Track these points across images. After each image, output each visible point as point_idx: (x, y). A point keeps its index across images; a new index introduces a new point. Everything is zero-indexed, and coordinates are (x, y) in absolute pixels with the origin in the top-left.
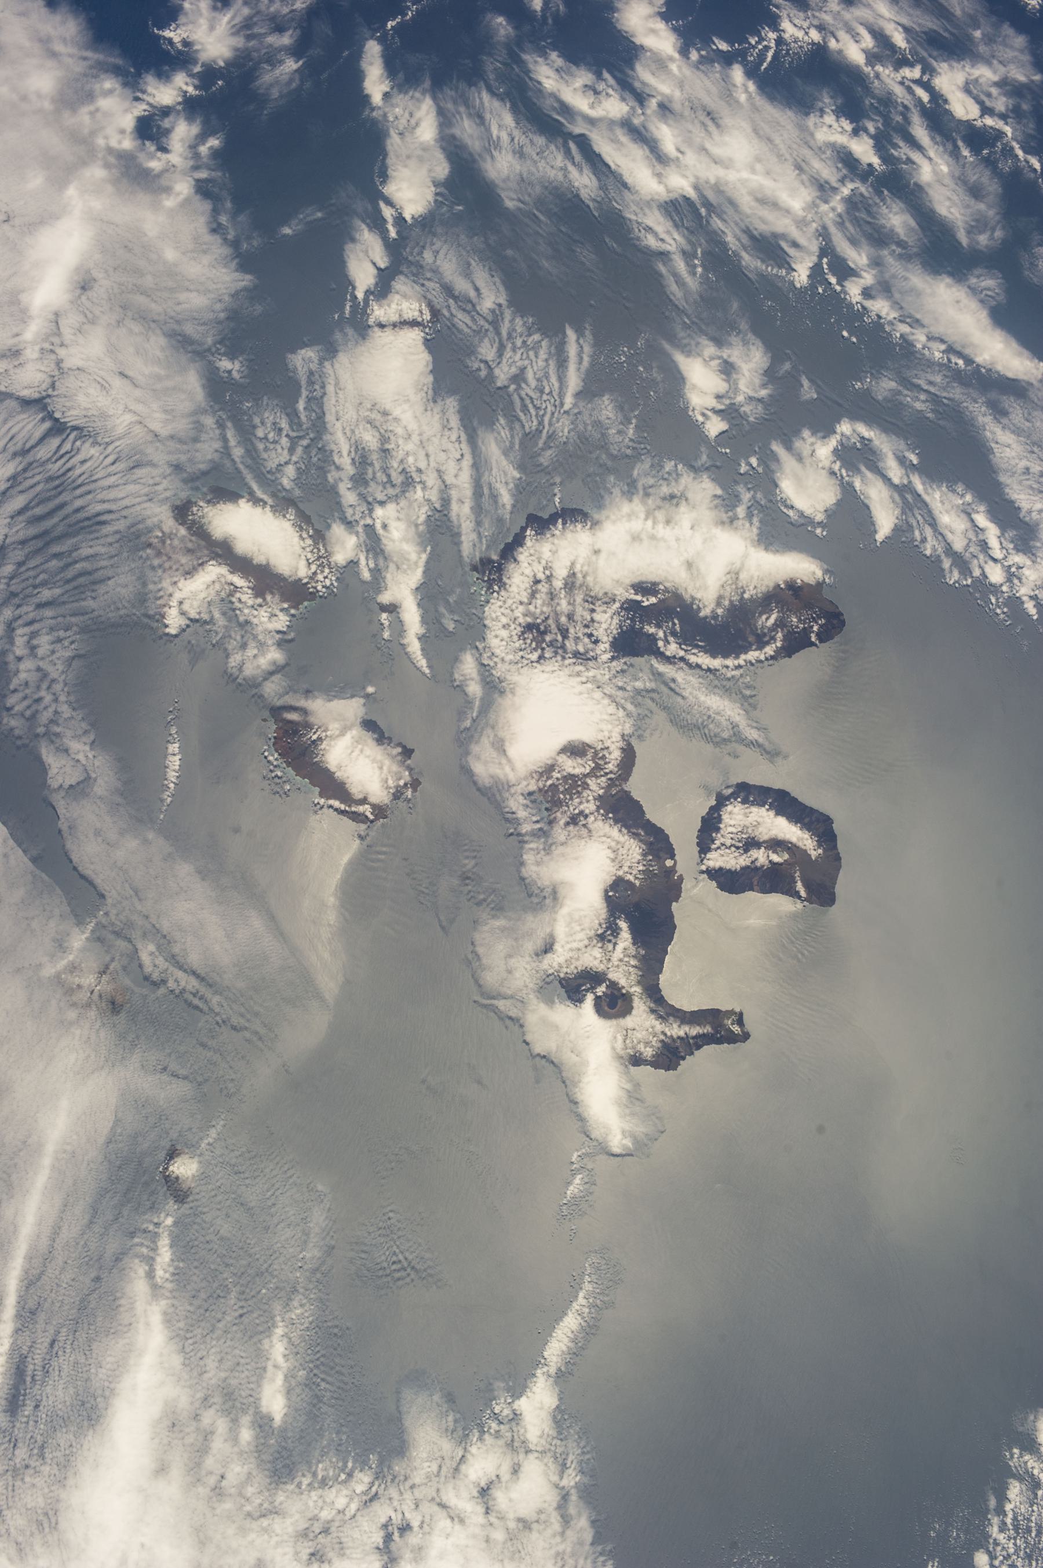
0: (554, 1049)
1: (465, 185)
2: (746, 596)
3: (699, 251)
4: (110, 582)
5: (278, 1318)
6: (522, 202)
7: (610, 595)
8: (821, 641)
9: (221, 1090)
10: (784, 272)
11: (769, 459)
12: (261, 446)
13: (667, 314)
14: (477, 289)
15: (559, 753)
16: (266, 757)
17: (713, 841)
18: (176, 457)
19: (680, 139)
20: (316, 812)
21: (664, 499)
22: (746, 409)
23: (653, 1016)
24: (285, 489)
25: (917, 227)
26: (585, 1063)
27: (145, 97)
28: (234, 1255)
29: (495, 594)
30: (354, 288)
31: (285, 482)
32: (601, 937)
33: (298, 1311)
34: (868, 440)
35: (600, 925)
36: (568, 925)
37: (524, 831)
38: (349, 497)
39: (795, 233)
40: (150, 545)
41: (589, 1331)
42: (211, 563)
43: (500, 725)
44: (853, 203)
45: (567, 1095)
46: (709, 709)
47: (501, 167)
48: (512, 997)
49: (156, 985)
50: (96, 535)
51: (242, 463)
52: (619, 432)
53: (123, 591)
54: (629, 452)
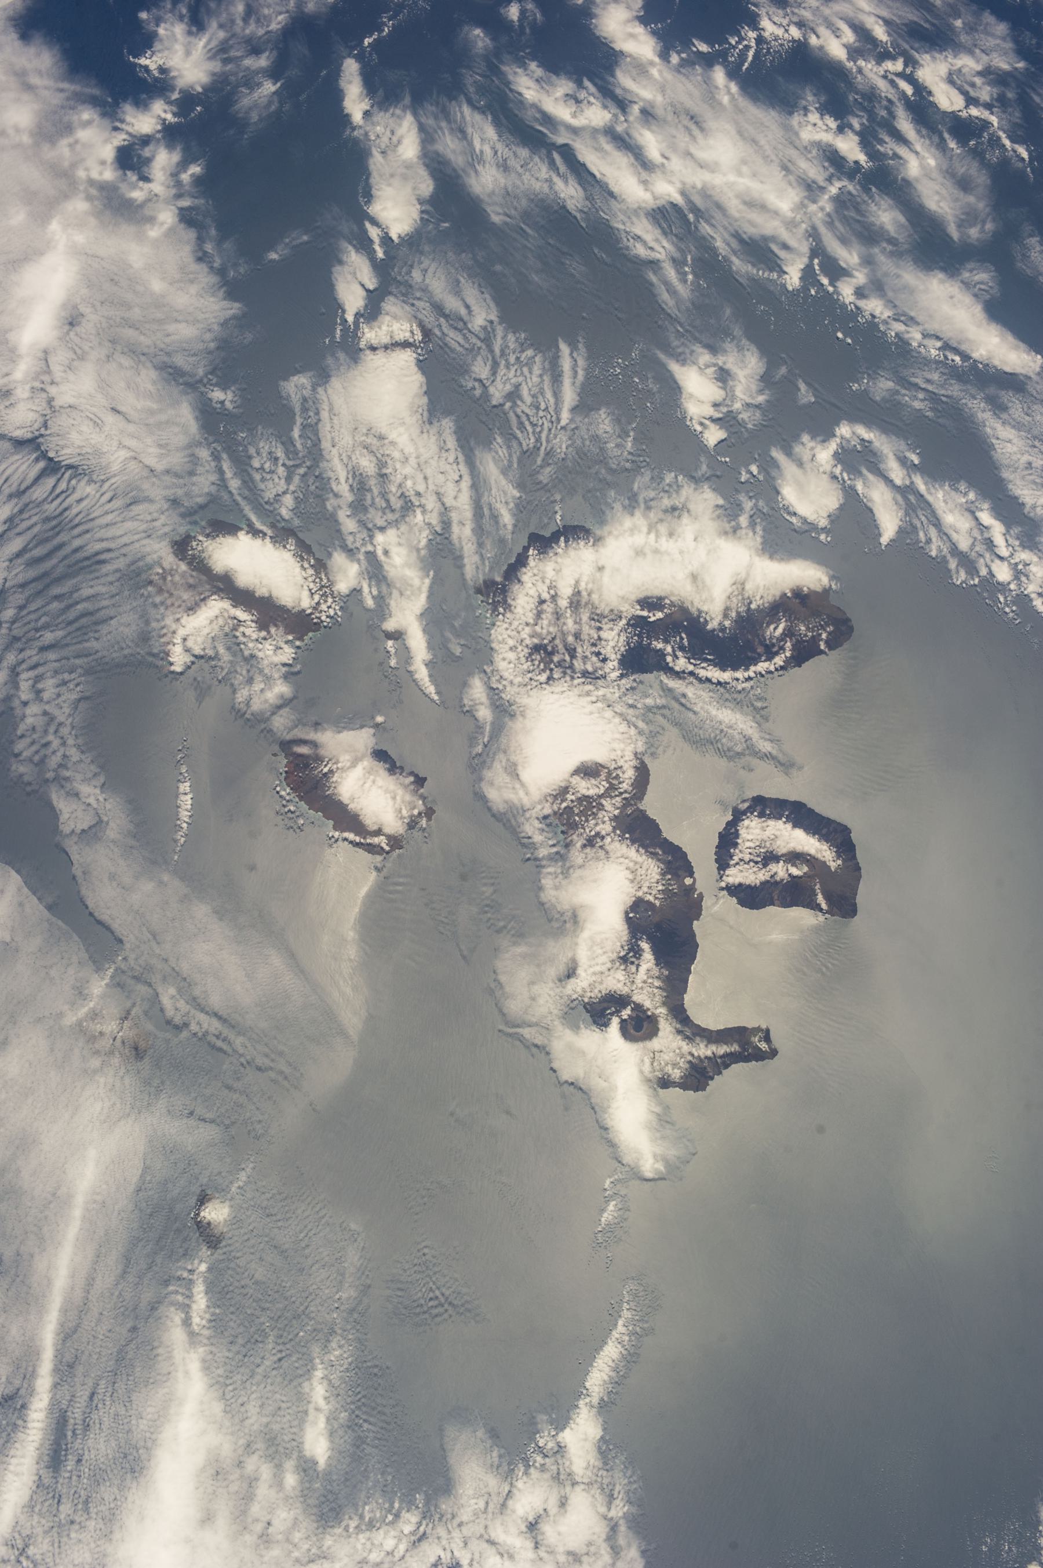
0: (582, 1075)
1: (450, 202)
2: (753, 606)
3: (689, 258)
4: (112, 622)
5: (317, 1361)
6: (509, 216)
7: (616, 612)
8: (830, 650)
9: (249, 1132)
10: (775, 275)
11: (769, 466)
12: (257, 477)
13: (660, 323)
14: (467, 307)
16: (278, 792)
17: (731, 857)
18: (173, 491)
19: (664, 145)
20: (331, 846)
21: (666, 511)
22: (744, 416)
23: (679, 1037)
24: (284, 520)
25: (907, 223)
27: (124, 126)
28: (270, 1299)
29: (501, 617)
30: (344, 311)
31: (284, 512)
32: (624, 960)
33: (337, 1353)
34: (869, 442)
35: (622, 947)
36: (590, 948)
37: (541, 856)
38: (349, 525)
39: (785, 235)
40: (151, 583)
41: (630, 1359)
42: (213, 597)
43: (512, 749)
44: (841, 201)
45: (597, 1121)
46: (721, 723)
47: (485, 181)
48: (537, 1024)
49: (178, 1028)
50: (97, 574)
51: (239, 494)
52: (617, 446)
53: (126, 631)
54: (628, 465)
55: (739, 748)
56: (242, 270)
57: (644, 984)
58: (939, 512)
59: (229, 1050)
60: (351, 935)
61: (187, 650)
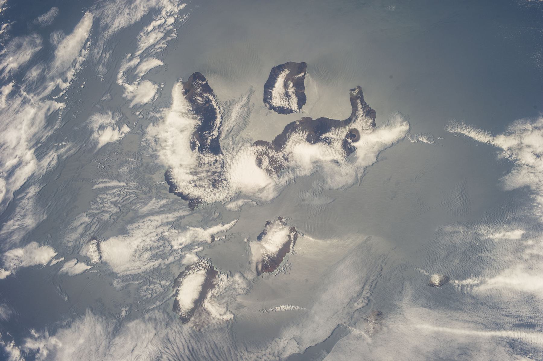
2: (191, 109)
5: (486, 237)
10: (60, 112)
11: (137, 107)
12: (155, 295)
14: (81, 224)
17: (288, 108)
21: (157, 144)
22: (117, 119)
26: (377, 142)
30: (87, 270)
31: (168, 284)
32: (329, 143)
34: (124, 72)
38: (171, 259)
39: (44, 110)
46: (237, 117)
48: (356, 172)
52: (132, 164)
54: (140, 159)
55: (246, 109)
56: (73, 310)
57: (337, 136)
58: (149, 45)
59: (376, 281)
60: (329, 242)
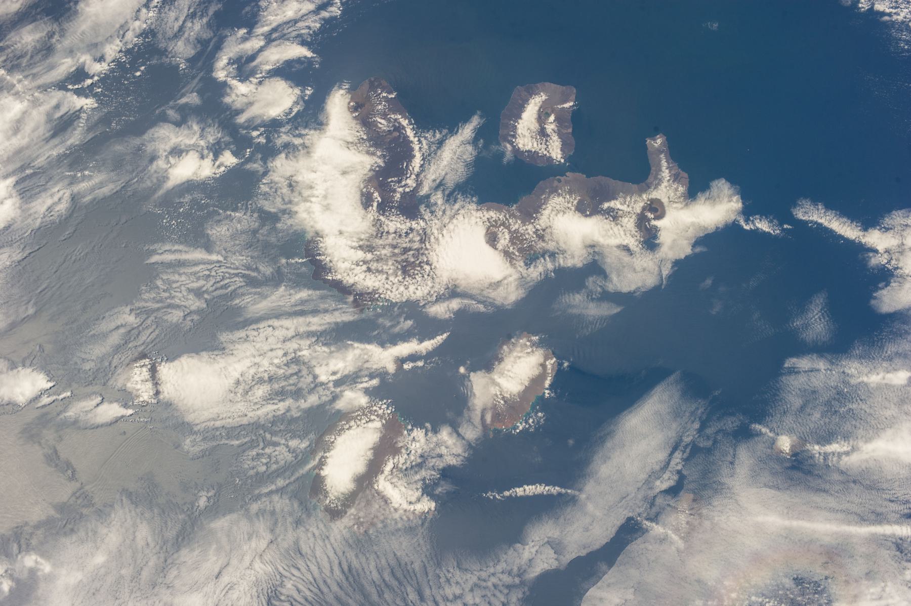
2: (365, 137)
10: (84, 116)
12: (274, 467)
14: (118, 328)
15: (496, 249)
21: (292, 191)
22: (211, 139)
26: (693, 224)
30: (122, 417)
31: (304, 445)
34: (230, 59)
36: (610, 237)
38: (313, 400)
46: (452, 159)
48: (660, 267)
52: (239, 222)
54: (256, 215)
61: (419, 500)
